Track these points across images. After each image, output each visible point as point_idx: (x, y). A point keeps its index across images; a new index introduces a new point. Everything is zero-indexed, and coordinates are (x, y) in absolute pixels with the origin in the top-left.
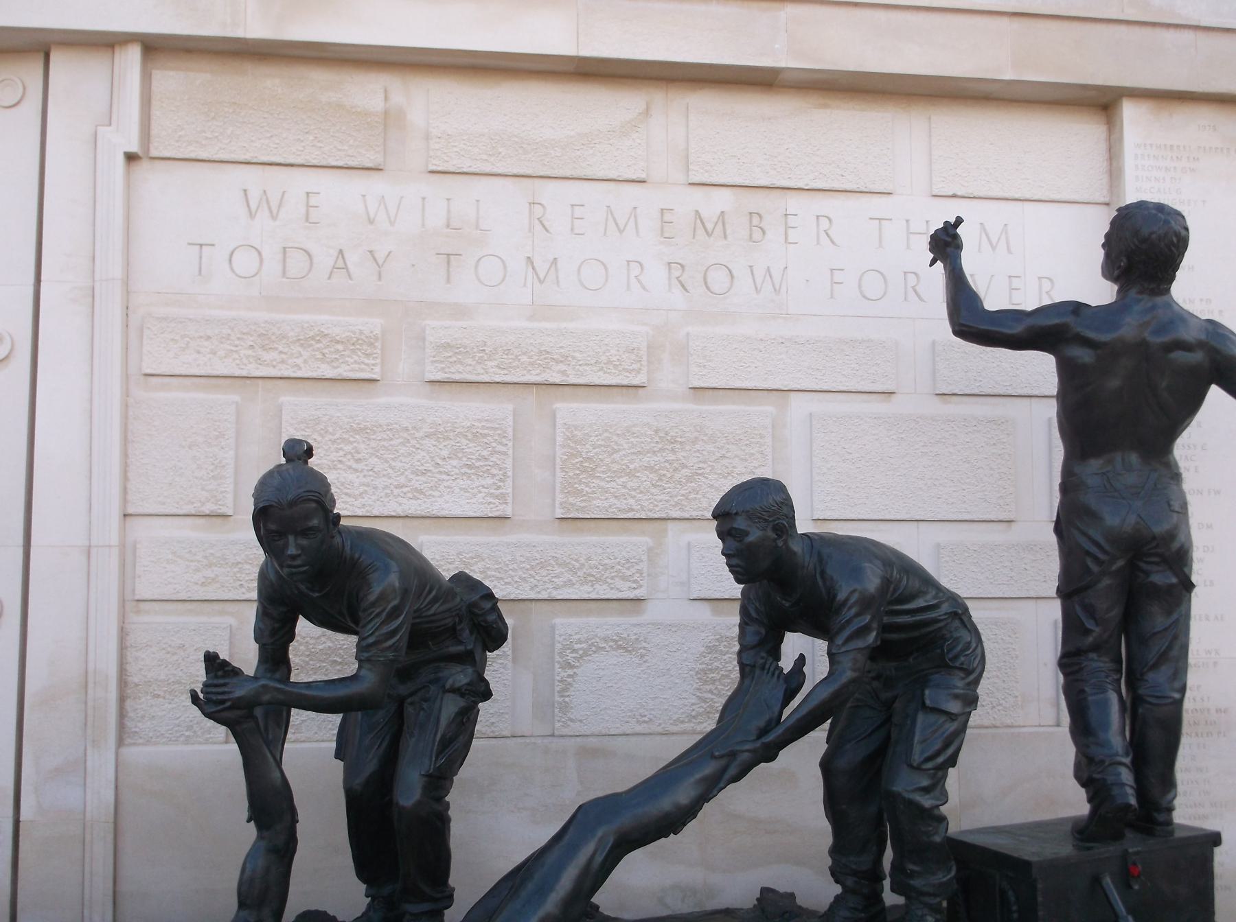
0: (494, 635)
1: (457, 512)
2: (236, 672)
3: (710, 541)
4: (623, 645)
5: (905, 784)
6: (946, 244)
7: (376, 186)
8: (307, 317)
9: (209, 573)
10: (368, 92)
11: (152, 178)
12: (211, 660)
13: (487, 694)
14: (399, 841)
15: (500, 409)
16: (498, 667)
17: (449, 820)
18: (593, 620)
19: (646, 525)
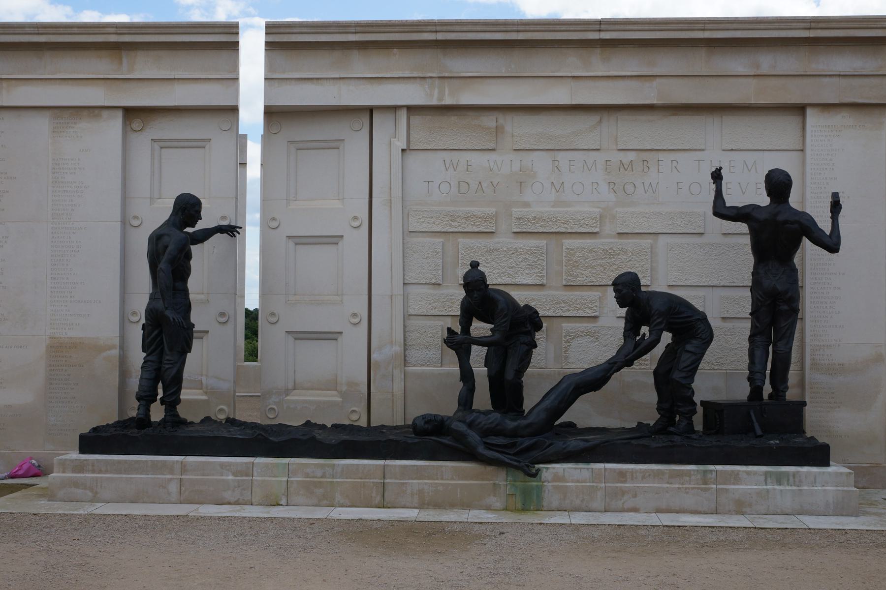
0: (538, 326)
1: (524, 282)
2: (457, 333)
3: (611, 293)
4: (589, 334)
5: (677, 375)
6: (717, 176)
7: (493, 156)
8: (467, 209)
9: (434, 305)
10: (490, 121)
11: (412, 158)
12: (449, 329)
13: (536, 346)
14: (506, 392)
15: (542, 242)
16: (539, 337)
17: (522, 387)
18: (577, 325)
19: (599, 288)
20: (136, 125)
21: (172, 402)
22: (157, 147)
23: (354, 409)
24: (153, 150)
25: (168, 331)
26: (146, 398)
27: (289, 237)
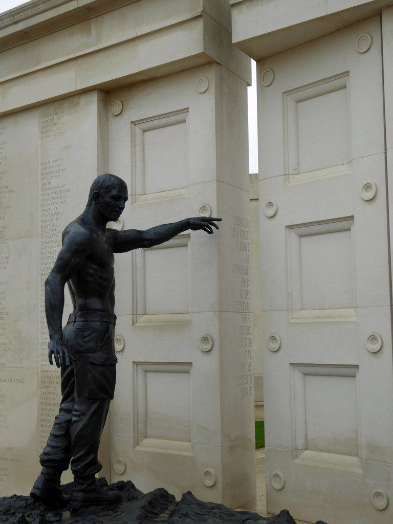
20: (116, 109)
21: (88, 471)
22: (138, 131)
23: (380, 490)
24: (133, 135)
25: (87, 367)
26: (52, 465)
27: (290, 227)
